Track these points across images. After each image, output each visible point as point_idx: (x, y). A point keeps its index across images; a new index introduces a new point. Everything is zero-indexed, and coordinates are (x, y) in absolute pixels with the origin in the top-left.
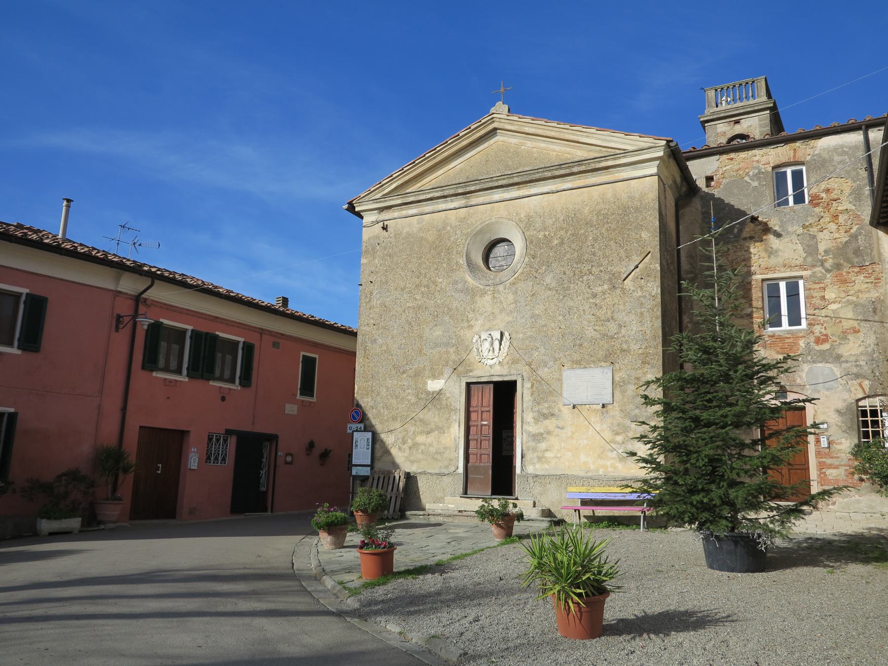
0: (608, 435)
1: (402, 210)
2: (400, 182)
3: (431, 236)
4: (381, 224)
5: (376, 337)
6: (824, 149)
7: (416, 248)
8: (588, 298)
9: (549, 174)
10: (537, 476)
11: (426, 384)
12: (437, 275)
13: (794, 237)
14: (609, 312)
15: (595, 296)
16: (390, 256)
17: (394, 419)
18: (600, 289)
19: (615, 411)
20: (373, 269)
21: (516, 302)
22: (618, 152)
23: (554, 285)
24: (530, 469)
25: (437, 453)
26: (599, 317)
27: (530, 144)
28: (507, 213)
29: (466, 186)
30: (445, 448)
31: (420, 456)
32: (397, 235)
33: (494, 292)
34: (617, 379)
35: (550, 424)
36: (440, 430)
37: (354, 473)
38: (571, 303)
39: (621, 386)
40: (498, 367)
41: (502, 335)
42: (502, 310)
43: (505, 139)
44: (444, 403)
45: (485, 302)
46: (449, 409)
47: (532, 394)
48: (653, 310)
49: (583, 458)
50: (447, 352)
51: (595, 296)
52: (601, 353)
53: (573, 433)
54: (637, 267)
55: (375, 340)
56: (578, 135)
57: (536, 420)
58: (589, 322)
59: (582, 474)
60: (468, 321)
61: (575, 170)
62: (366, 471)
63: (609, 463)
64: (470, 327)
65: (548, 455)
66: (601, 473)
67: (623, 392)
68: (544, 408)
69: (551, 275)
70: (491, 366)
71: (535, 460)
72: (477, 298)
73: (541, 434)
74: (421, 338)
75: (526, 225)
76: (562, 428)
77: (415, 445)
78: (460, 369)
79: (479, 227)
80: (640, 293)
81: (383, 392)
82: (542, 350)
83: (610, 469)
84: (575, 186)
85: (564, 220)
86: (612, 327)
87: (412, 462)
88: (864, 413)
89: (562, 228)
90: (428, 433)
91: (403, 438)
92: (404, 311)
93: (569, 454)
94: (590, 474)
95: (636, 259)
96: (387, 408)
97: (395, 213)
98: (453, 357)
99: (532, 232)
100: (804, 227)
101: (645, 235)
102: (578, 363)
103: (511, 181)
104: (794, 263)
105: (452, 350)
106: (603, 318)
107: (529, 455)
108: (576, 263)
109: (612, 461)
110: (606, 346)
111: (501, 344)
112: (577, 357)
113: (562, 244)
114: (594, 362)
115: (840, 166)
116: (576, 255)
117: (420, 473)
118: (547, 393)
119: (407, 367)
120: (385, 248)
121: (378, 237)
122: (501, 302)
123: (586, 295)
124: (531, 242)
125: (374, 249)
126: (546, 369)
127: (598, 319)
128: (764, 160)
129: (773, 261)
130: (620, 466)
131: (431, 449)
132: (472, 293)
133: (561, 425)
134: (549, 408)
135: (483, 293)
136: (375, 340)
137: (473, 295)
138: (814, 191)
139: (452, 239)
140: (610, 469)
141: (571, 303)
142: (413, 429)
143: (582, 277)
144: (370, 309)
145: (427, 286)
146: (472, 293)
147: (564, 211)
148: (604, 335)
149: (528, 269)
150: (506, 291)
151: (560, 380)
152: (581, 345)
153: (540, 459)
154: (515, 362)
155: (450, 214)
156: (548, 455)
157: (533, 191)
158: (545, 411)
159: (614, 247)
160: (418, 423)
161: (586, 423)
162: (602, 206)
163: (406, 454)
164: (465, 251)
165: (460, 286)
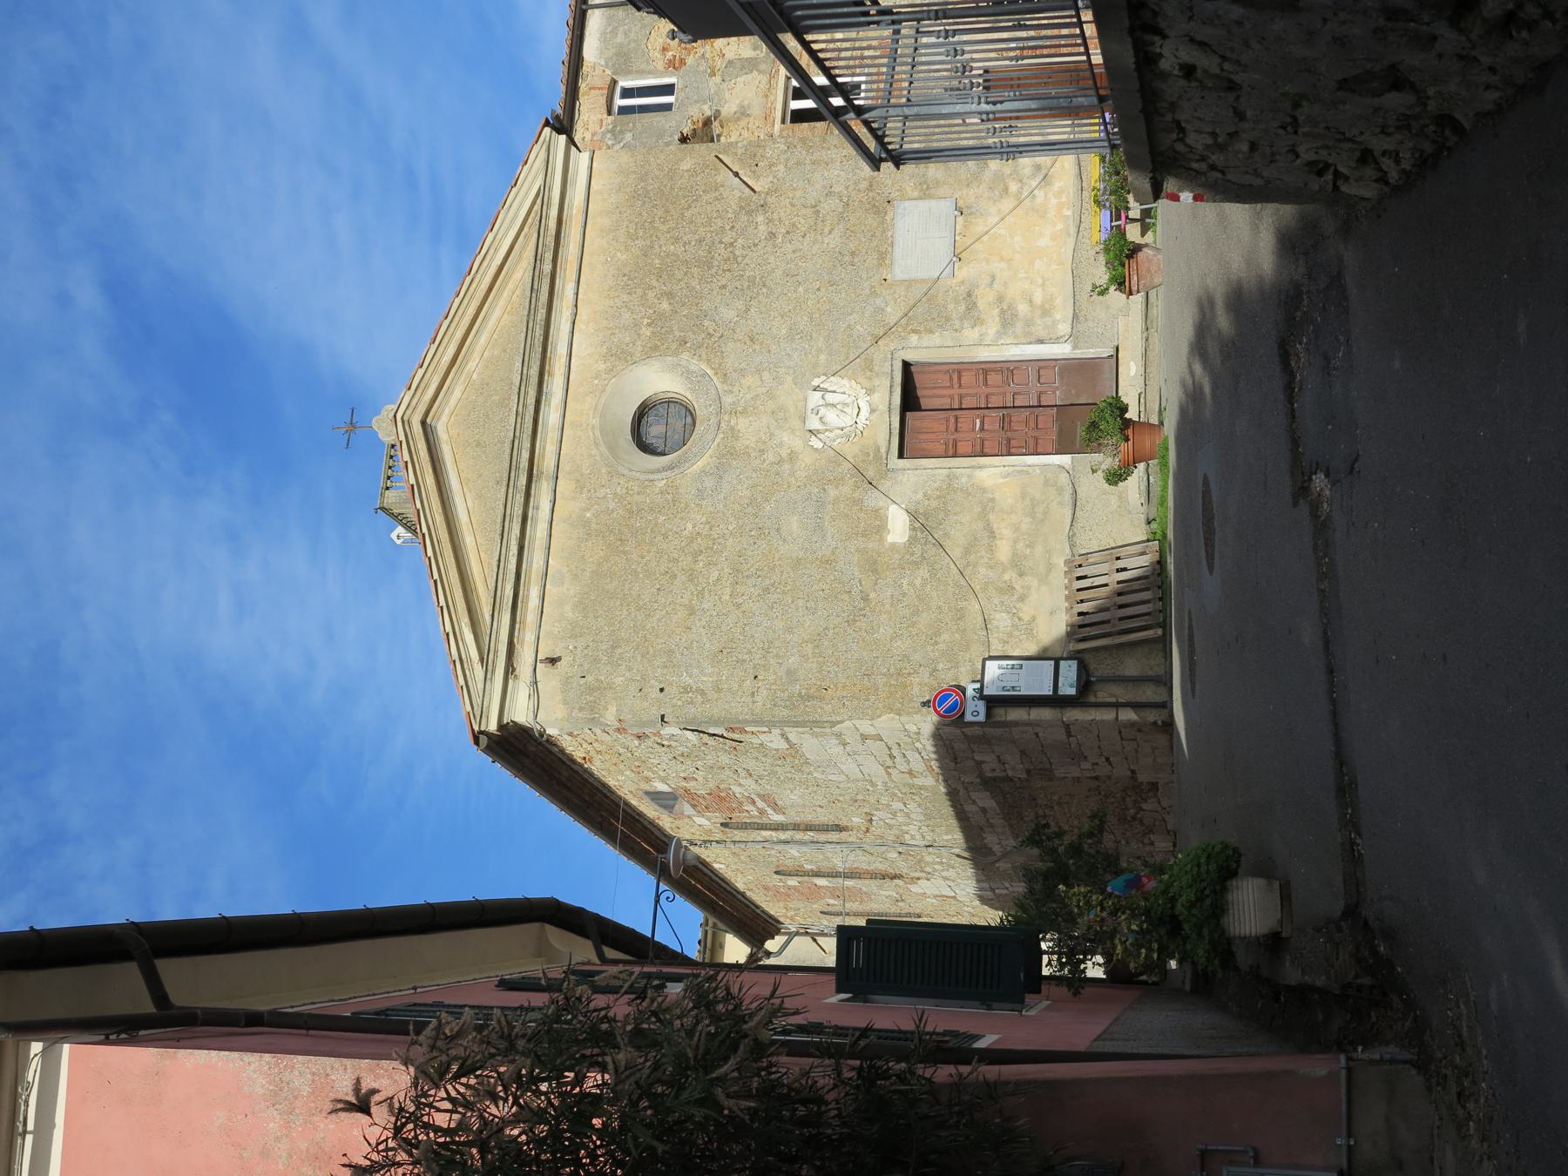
0: (1007, 204)
1: (523, 622)
5: (782, 672)
6: (601, 53)
9: (542, 313)
10: (1075, 316)
11: (893, 545)
13: (724, 85)
14: (804, 211)
15: (772, 235)
16: (614, 647)
17: (960, 615)
18: (762, 228)
19: (969, 195)
20: (633, 688)
21: (759, 371)
22: (537, 207)
23: (740, 304)
24: (1064, 328)
25: (1032, 514)
27: (473, 365)
29: (518, 468)
30: (1024, 496)
31: (1039, 550)
34: (916, 194)
35: (985, 298)
36: (988, 507)
37: (1072, 691)
38: (779, 272)
40: (876, 397)
42: (770, 395)
43: (447, 411)
44: (934, 504)
45: (749, 429)
46: (950, 487)
47: (931, 332)
49: (1044, 242)
50: (836, 500)
51: (772, 235)
53: (1002, 259)
54: (736, 174)
55: (789, 673)
56: (489, 266)
57: (978, 321)
59: (1071, 241)
60: (780, 462)
61: (547, 268)
62: (1069, 670)
63: (1054, 201)
64: (792, 457)
65: (1038, 298)
66: (1069, 213)
67: (937, 184)
69: (722, 309)
70: (873, 411)
71: (1048, 320)
72: (739, 445)
73: (1003, 312)
74: (799, 561)
75: (619, 357)
76: (993, 278)
77: (1017, 564)
78: (870, 474)
79: (603, 449)
80: (781, 167)
82: (853, 318)
84: (574, 277)
86: (830, 206)
87: (1050, 567)
90: (992, 535)
91: (1001, 591)
92: (738, 606)
93: (1038, 263)
94: (1073, 231)
96: (937, 634)
97: (527, 639)
98: (846, 490)
100: (713, 74)
101: (687, 165)
102: (884, 257)
104: (764, 85)
109: (1050, 195)
112: (872, 260)
113: (670, 295)
115: (632, 36)
116: (695, 271)
117: (1072, 546)
118: (928, 305)
120: (596, 660)
121: (567, 682)
124: (655, 348)
125: (590, 690)
128: (594, 127)
129: (757, 111)
130: (1057, 185)
131: (1024, 527)
132: (728, 454)
133: (987, 280)
134: (956, 301)
135: (733, 433)
136: (789, 673)
138: (660, 65)
140: (1064, 199)
142: (983, 571)
143: (735, 258)
144: (719, 690)
145: (696, 555)
147: (613, 294)
148: (841, 217)
150: (735, 389)
151: (909, 283)
152: (853, 254)
153: (1046, 312)
154: (869, 367)
155: (561, 511)
156: (1038, 298)
158: (962, 308)
159: (694, 210)
160: (972, 558)
161: (985, 238)
163: (1035, 583)
164: (643, 477)
165: (709, 483)
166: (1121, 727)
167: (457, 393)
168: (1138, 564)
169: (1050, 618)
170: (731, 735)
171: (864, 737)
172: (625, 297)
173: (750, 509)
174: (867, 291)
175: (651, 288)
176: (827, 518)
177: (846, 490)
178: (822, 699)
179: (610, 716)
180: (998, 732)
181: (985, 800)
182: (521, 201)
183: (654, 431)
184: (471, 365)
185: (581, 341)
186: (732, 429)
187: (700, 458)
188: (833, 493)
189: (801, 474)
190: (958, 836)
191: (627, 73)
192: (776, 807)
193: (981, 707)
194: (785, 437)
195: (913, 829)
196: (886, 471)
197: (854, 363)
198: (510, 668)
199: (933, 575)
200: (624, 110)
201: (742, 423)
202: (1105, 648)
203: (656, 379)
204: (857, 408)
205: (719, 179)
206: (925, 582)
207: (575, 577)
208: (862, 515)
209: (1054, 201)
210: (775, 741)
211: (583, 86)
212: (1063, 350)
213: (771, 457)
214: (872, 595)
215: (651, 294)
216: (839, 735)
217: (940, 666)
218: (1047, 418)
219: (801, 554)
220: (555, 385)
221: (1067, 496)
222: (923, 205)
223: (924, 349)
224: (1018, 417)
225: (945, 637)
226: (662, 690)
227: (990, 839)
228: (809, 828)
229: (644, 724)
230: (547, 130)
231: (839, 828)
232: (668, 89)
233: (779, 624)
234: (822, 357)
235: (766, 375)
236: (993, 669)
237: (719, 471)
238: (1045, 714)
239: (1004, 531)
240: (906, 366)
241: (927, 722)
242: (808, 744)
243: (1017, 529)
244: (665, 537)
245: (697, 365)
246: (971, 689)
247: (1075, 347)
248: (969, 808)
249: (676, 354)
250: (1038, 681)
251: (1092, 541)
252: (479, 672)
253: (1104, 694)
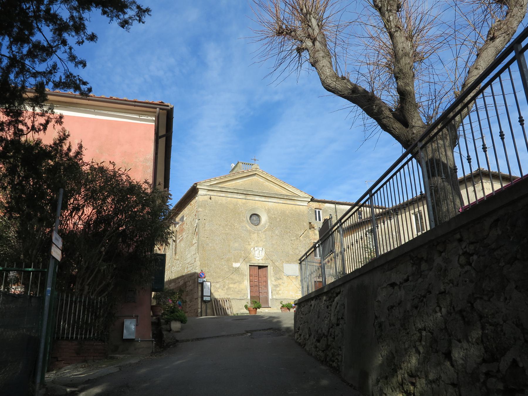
2: (218, 182)
9: (277, 196)
15: (292, 240)
17: (219, 277)
24: (274, 297)
27: (267, 183)
28: (264, 207)
31: (232, 292)
35: (280, 282)
36: (240, 282)
42: (261, 240)
50: (241, 253)
51: (292, 240)
57: (276, 280)
60: (249, 242)
62: (208, 299)
64: (249, 245)
68: (278, 276)
72: (252, 234)
75: (268, 211)
77: (229, 288)
78: (246, 260)
81: (213, 266)
87: (228, 295)
90: (234, 283)
91: (224, 285)
98: (243, 255)
102: (288, 262)
103: (264, 195)
105: (243, 252)
107: (274, 292)
112: (287, 260)
113: (280, 221)
118: (278, 271)
119: (224, 257)
120: (210, 207)
121: (207, 201)
125: (205, 206)
132: (250, 232)
137: (250, 233)
146: (250, 232)
151: (283, 267)
153: (277, 293)
155: (239, 200)
156: (280, 292)
157: (270, 200)
166: (197, 309)
167: (261, 180)
168: (229, 312)
169: (218, 295)
170: (196, 232)
171: (195, 259)
177: (243, 255)
179: (200, 209)
180: (196, 285)
181: (182, 283)
182: (298, 192)
183: (254, 218)
184: (267, 183)
185: (272, 204)
187: (249, 227)
190: (173, 278)
191: (323, 212)
192: (180, 241)
193: (201, 281)
195: (175, 268)
196: (247, 263)
197: (268, 256)
198: (209, 190)
200: (316, 211)
201: (256, 235)
202: (213, 306)
203: (264, 218)
204: (259, 256)
210: (194, 241)
211: (320, 203)
212: (270, 297)
216: (195, 254)
218: (257, 294)
220: (263, 199)
221: (242, 298)
223: (270, 269)
224: (257, 288)
227: (173, 284)
228: (176, 248)
229: (198, 216)
231: (175, 254)
232: (320, 220)
236: (209, 284)
238: (200, 294)
239: (235, 286)
240: (267, 266)
241: (198, 271)
242: (194, 248)
243: (236, 288)
245: (267, 226)
246: (205, 279)
248: (180, 280)
250: (206, 293)
251: (233, 303)
252: (209, 184)
253: (204, 306)
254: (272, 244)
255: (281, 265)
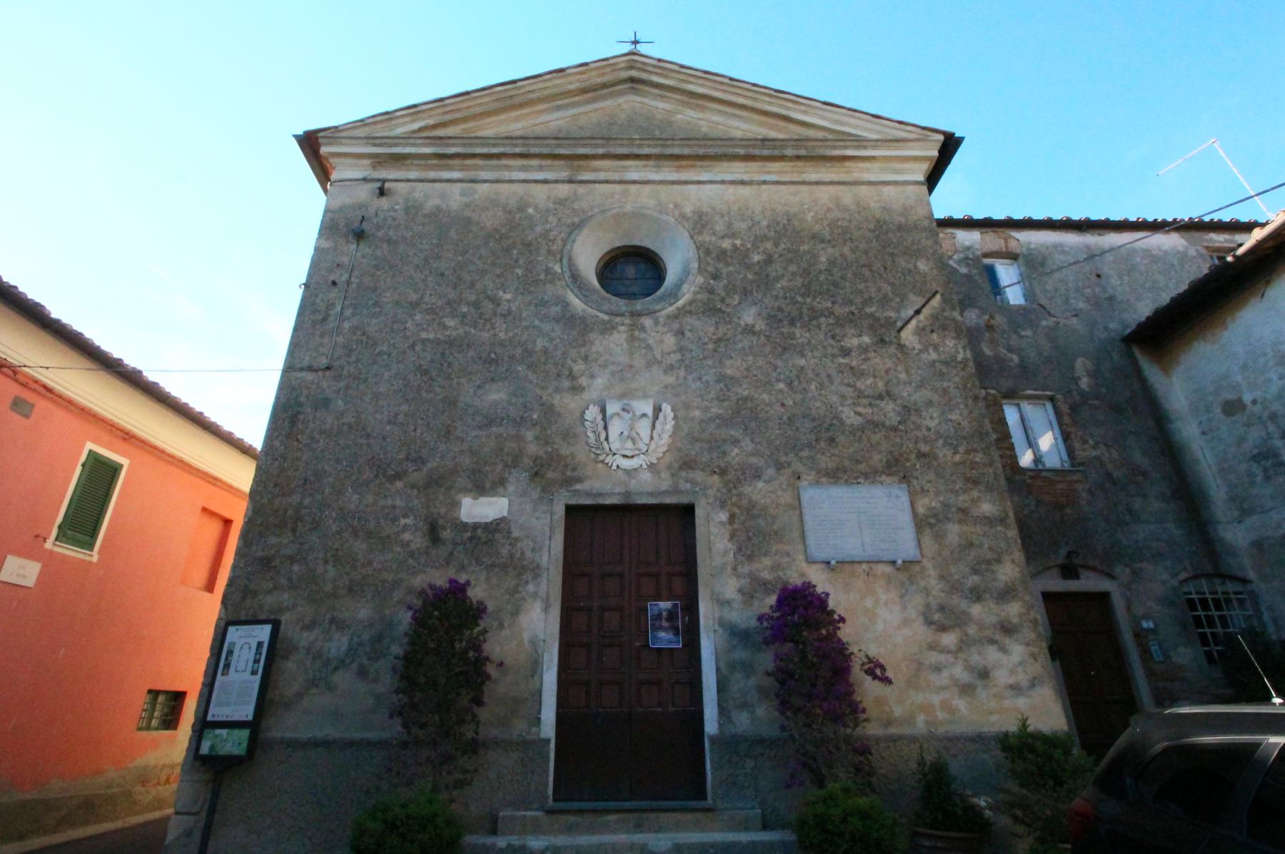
3: (490, 220)
4: (379, 185)
7: (453, 234)
8: (834, 356)
11: (456, 505)
12: (503, 287)
15: (846, 352)
18: (855, 341)
21: (681, 350)
26: (861, 391)
32: (412, 209)
33: (633, 327)
34: (921, 510)
38: (802, 362)
39: (931, 526)
40: (646, 476)
41: (657, 410)
43: (646, 100)
44: (505, 552)
46: (522, 569)
47: (732, 536)
48: (965, 386)
50: (518, 438)
51: (846, 352)
52: (877, 457)
54: (918, 312)
56: (788, 108)
58: (843, 397)
60: (572, 377)
64: (576, 389)
67: (939, 537)
69: (753, 310)
72: (593, 336)
75: (700, 222)
82: (748, 445)
83: (941, 715)
85: (768, 226)
86: (890, 411)
88: (1191, 604)
89: (765, 238)
92: (413, 346)
95: (917, 301)
96: (337, 560)
98: (533, 449)
99: (706, 238)
105: (530, 435)
106: (869, 392)
108: (802, 295)
109: (944, 695)
110: (885, 446)
111: (653, 427)
112: (825, 461)
113: (769, 260)
114: (866, 476)
122: (649, 347)
123: (829, 350)
124: (708, 252)
126: (760, 484)
127: (860, 394)
130: (961, 704)
134: (776, 567)
135: (608, 328)
139: (539, 229)
141: (802, 362)
144: (322, 335)
147: (768, 213)
149: (704, 296)
150: (660, 328)
151: (797, 506)
152: (832, 440)
162: (840, 215)
165: (555, 310)
167: (661, 105)
172: (764, 223)
173: (519, 351)
174: (783, 459)
175: (776, 244)
176: (501, 430)
178: (288, 436)
186: (614, 328)
188: (530, 435)
189: (556, 399)
194: (599, 382)
196: (547, 490)
199: (412, 554)
203: (678, 258)
205: (912, 297)
206: (406, 544)
207: (467, 205)
208: (499, 467)
209: (936, 699)
213: (578, 367)
214: (399, 484)
215: (769, 245)
217: (296, 568)
219: (461, 405)
222: (905, 519)
225: (331, 572)
226: (334, 283)
230: (941, 138)
233: (383, 389)
234: (697, 413)
235: (675, 357)
237: (569, 320)
244: (498, 276)
247: (713, 740)
249: (701, 270)
254: (722, 378)
255: (787, 498)
